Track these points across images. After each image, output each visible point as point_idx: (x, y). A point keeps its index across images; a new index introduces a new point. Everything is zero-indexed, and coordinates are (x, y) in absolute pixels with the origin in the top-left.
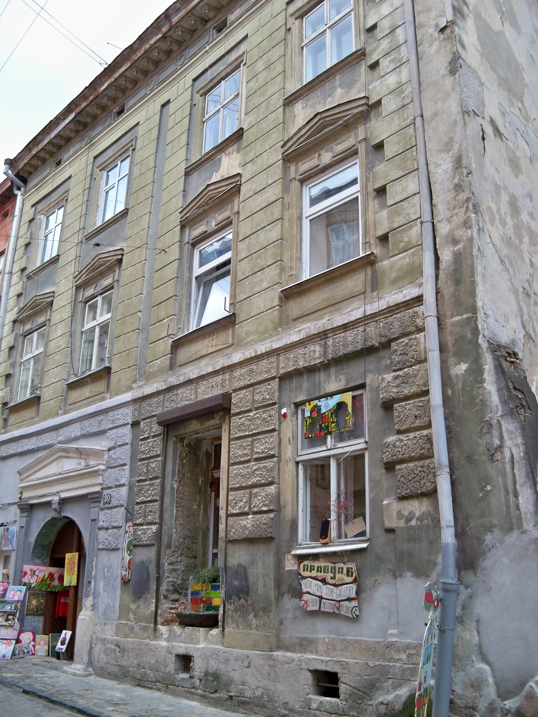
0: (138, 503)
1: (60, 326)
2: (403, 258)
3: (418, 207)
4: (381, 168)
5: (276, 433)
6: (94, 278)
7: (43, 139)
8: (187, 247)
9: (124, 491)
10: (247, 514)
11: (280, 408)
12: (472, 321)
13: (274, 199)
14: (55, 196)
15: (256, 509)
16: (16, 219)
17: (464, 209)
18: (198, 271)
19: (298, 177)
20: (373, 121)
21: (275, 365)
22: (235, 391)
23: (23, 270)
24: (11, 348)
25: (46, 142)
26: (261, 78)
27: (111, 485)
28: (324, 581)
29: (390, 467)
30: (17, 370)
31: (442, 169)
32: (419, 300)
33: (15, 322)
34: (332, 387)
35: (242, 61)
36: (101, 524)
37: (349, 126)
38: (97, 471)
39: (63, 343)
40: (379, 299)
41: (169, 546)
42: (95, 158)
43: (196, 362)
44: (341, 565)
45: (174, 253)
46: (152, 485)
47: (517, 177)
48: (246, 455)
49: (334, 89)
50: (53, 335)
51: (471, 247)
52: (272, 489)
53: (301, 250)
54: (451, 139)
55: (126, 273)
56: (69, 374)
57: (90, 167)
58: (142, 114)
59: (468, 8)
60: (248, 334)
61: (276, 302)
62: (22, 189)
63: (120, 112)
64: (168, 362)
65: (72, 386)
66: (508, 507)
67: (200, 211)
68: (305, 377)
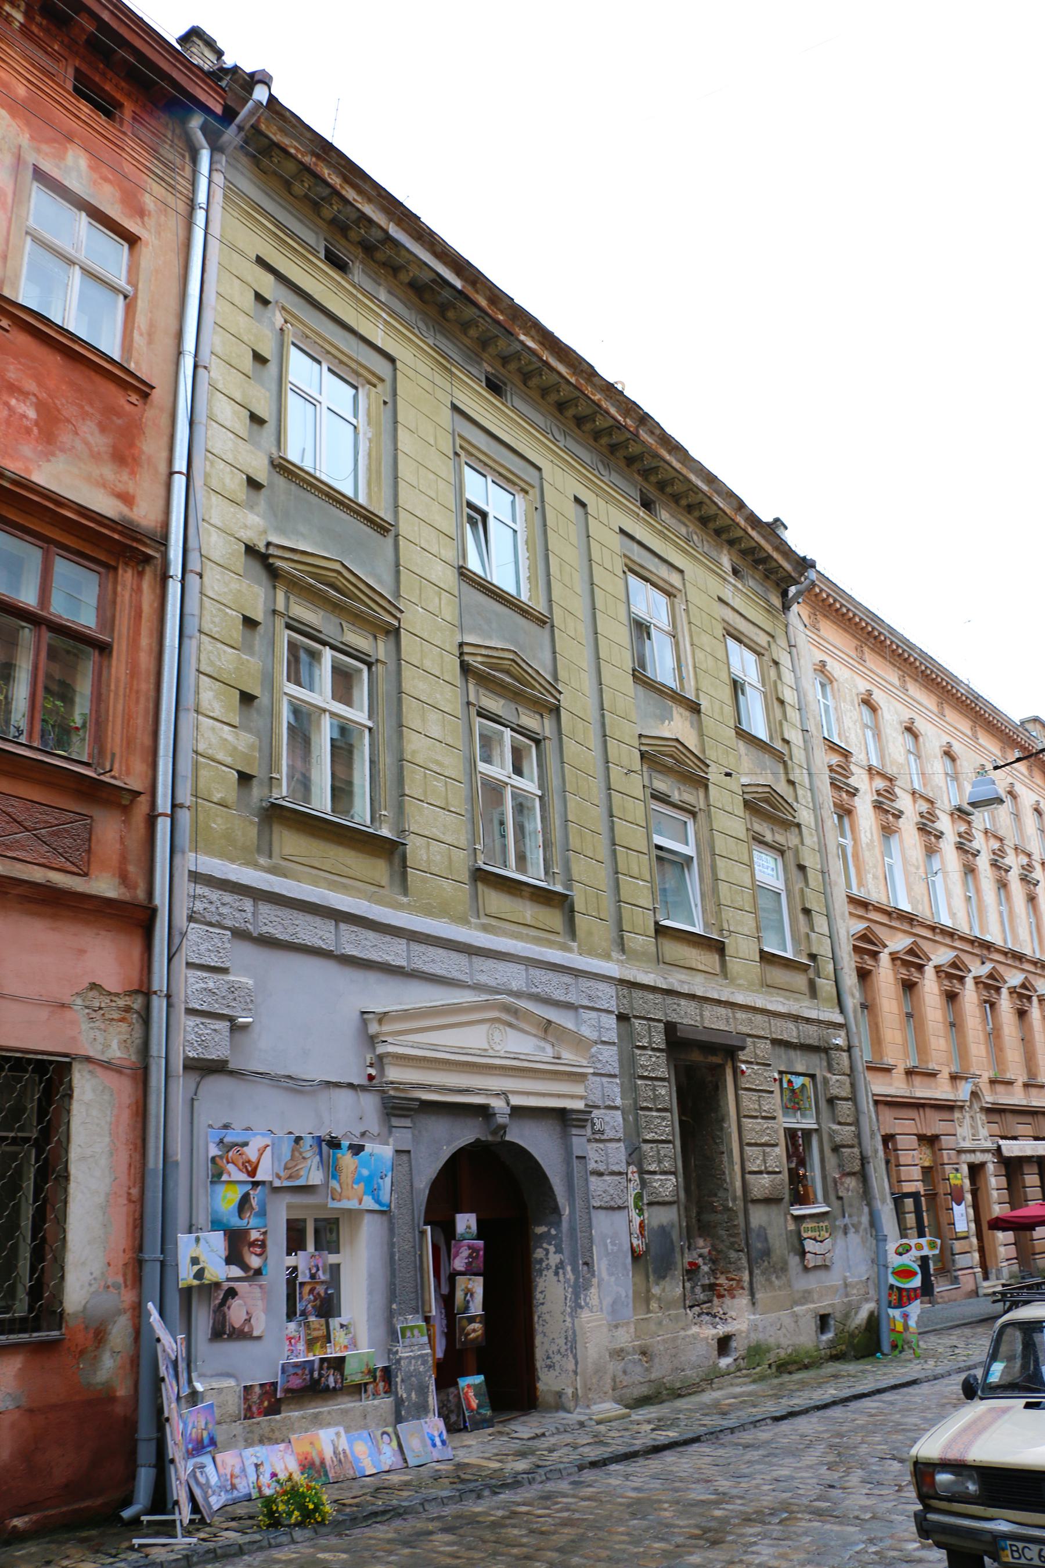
6: (503, 687)
15: (770, 1169)
27: (600, 1103)
33: (250, 550)
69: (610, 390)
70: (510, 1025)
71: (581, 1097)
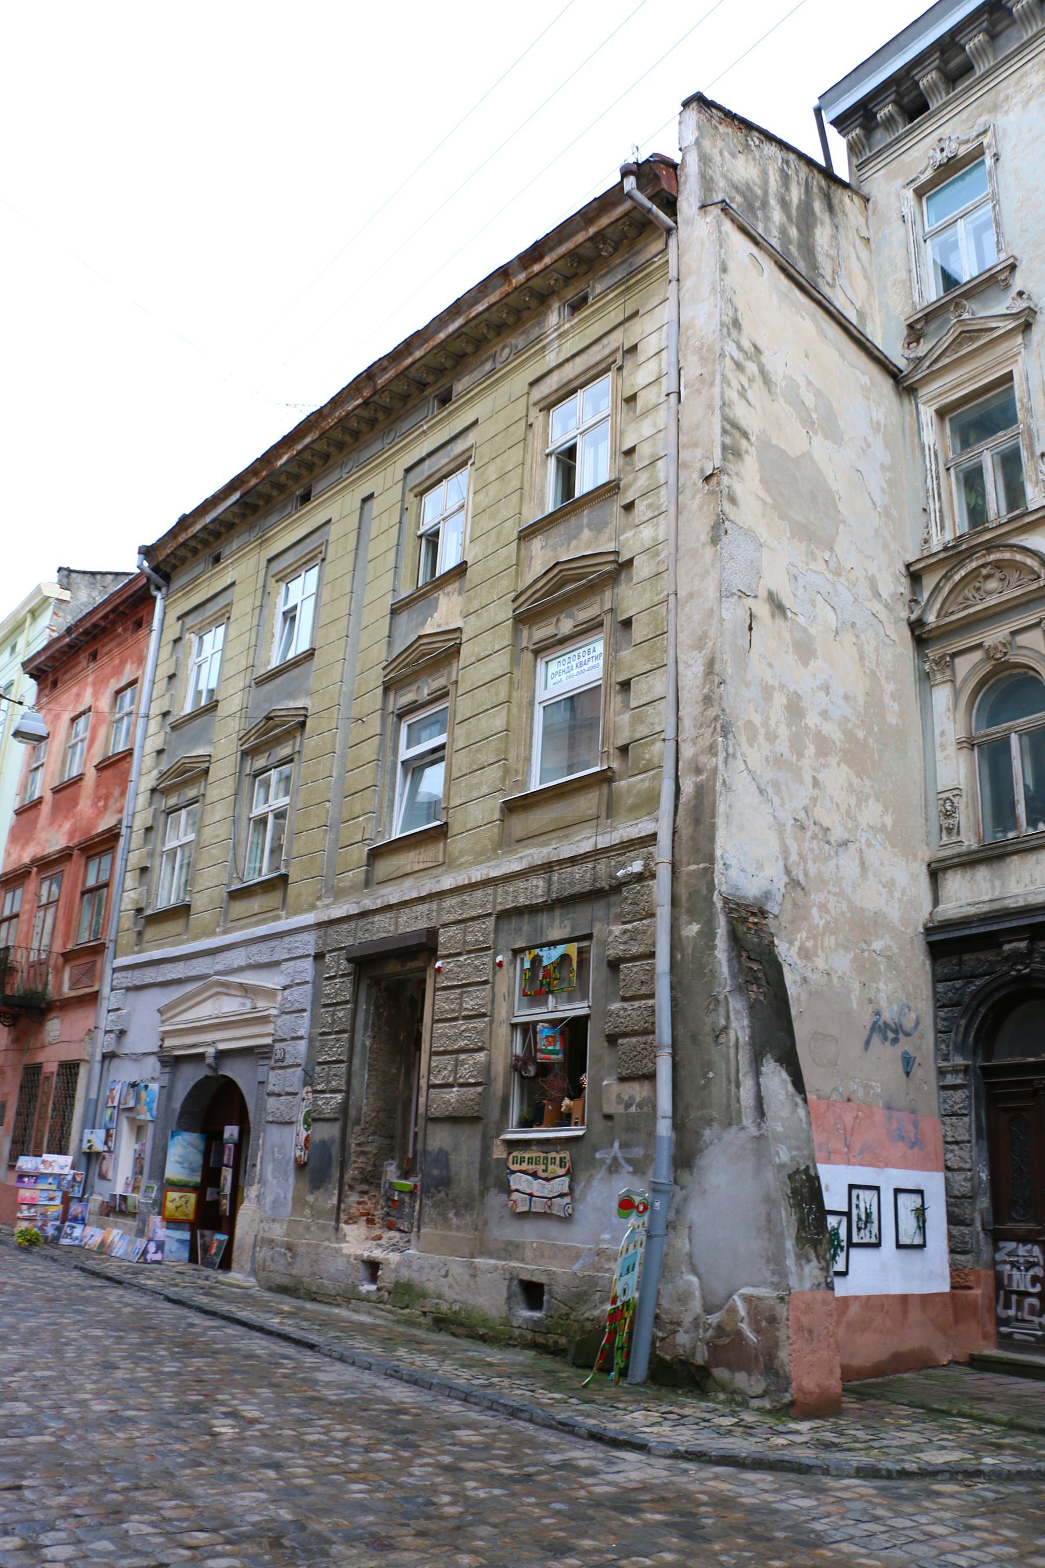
0: (320, 1064)
1: (219, 806)
2: (642, 780)
3: (662, 718)
4: (626, 654)
5: (488, 986)
7: (194, 523)
8: (391, 719)
9: (302, 1045)
10: (451, 1086)
11: (496, 954)
12: (709, 872)
13: (501, 673)
14: (212, 609)
15: (461, 1080)
16: (154, 635)
17: (711, 729)
18: (405, 753)
19: (532, 647)
20: (623, 587)
21: (491, 898)
22: (444, 926)
23: (165, 714)
24: (148, 830)
25: (198, 527)
26: (493, 490)
28: (534, 1175)
29: (612, 1039)
30: (157, 863)
31: (692, 672)
32: (653, 837)
33: (153, 791)
34: (556, 934)
35: (470, 457)
36: (270, 1088)
37: (594, 588)
38: (267, 1017)
39: (223, 831)
40: (614, 829)
41: (357, 1122)
42: (270, 561)
43: (398, 881)
44: (553, 1154)
45: (374, 724)
46: (338, 1040)
47: (806, 664)
48: (453, 1010)
49: (580, 528)
50: (209, 819)
51: (715, 780)
52: (481, 1056)
53: (531, 746)
54: (705, 635)
55: (311, 742)
56: (231, 878)
57: (262, 573)
58: (336, 507)
59: (748, 439)
60: (462, 853)
61: (497, 815)
62: (164, 590)
63: (306, 498)
64: (363, 877)
65: (236, 895)
66: (729, 1099)
67: (409, 671)
68: (526, 917)
69: (335, 402)
70: (227, 994)
71: (268, 1035)
